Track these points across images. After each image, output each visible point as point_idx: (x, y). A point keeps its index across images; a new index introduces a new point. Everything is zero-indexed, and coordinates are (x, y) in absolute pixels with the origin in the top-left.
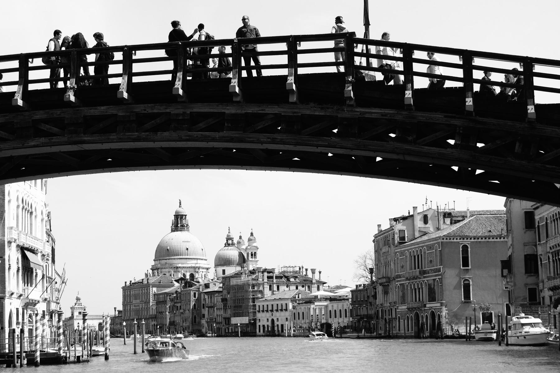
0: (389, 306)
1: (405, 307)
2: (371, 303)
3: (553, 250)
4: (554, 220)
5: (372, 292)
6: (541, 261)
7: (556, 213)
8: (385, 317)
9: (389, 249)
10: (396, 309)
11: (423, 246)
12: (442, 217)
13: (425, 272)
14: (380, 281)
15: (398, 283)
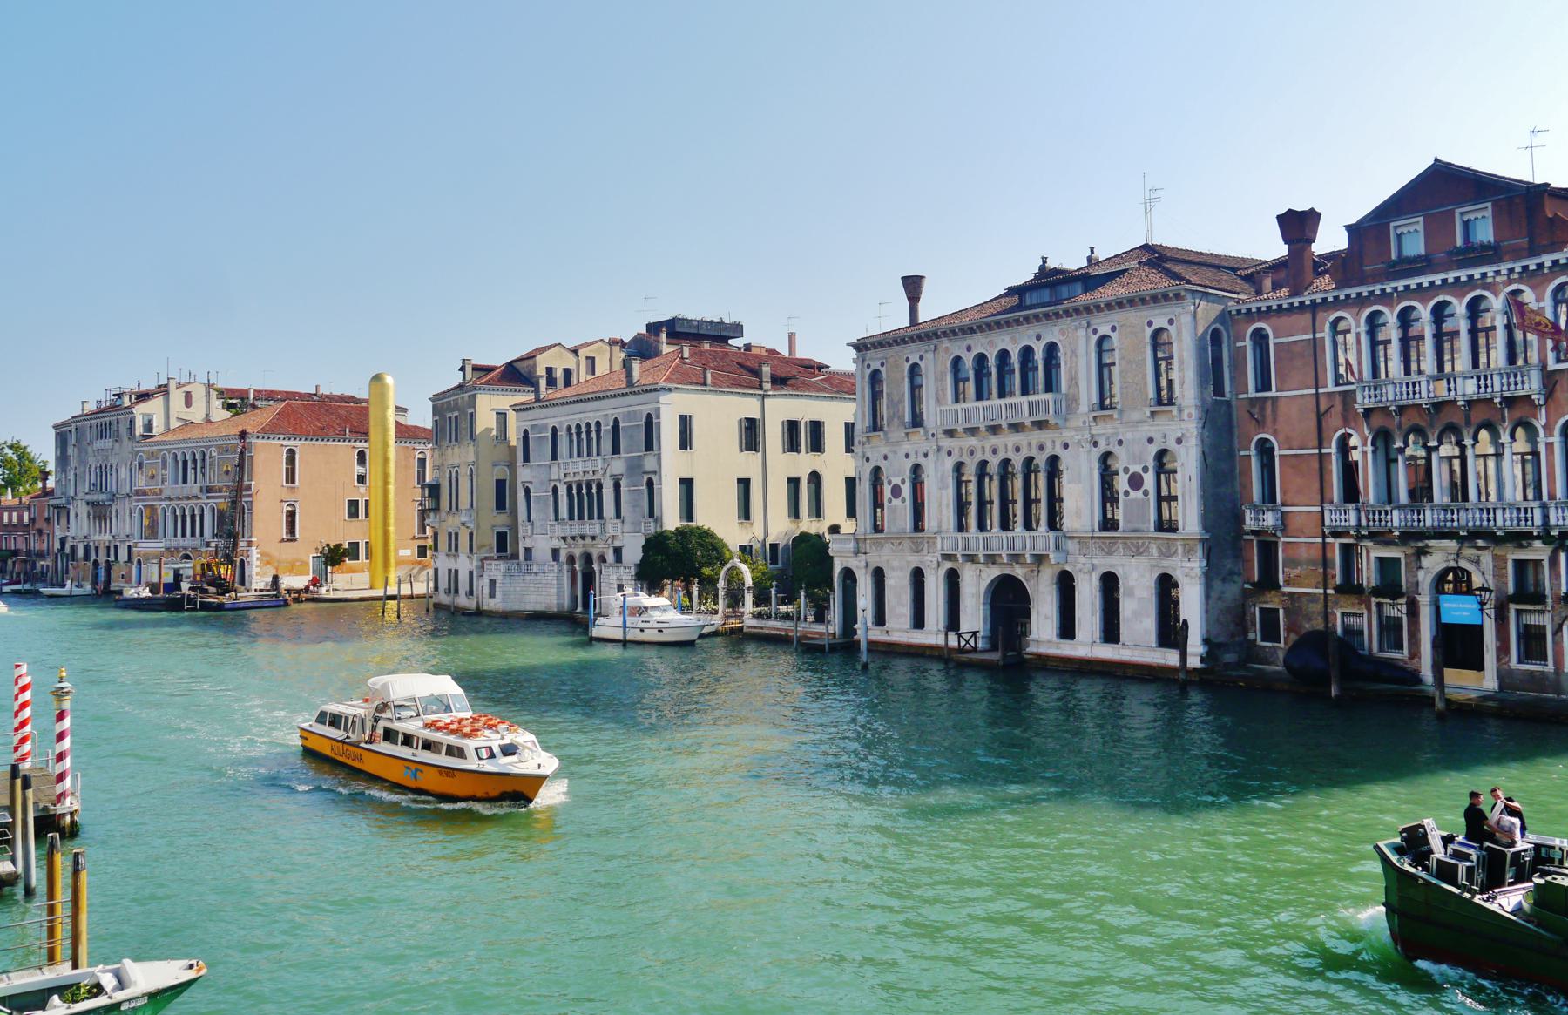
0: (110, 542)
1: (162, 545)
2: (40, 532)
3: (568, 479)
4: (579, 433)
5: (43, 511)
6: (527, 491)
7: (588, 425)
8: (92, 560)
9: (117, 446)
10: (129, 547)
11: (210, 446)
12: (215, 396)
13: (209, 490)
14: (88, 497)
15: (140, 503)
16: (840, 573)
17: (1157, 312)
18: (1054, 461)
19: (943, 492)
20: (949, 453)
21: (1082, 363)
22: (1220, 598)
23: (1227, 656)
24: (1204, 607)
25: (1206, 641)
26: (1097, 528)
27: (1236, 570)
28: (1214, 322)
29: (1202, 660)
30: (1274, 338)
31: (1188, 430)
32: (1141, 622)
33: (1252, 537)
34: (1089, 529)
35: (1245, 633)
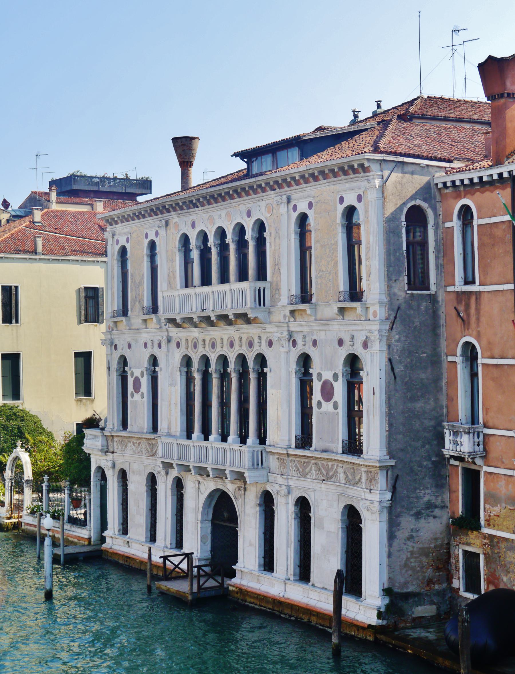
16: (94, 473)
17: (348, 185)
18: (262, 360)
19: (173, 388)
20: (178, 345)
21: (284, 244)
22: (411, 538)
23: (420, 608)
24: (386, 549)
25: (387, 592)
26: (293, 445)
27: (438, 502)
28: (413, 198)
29: (380, 615)
30: (479, 218)
31: (371, 332)
32: (329, 561)
33: (457, 463)
34: (286, 443)
35: (449, 579)
